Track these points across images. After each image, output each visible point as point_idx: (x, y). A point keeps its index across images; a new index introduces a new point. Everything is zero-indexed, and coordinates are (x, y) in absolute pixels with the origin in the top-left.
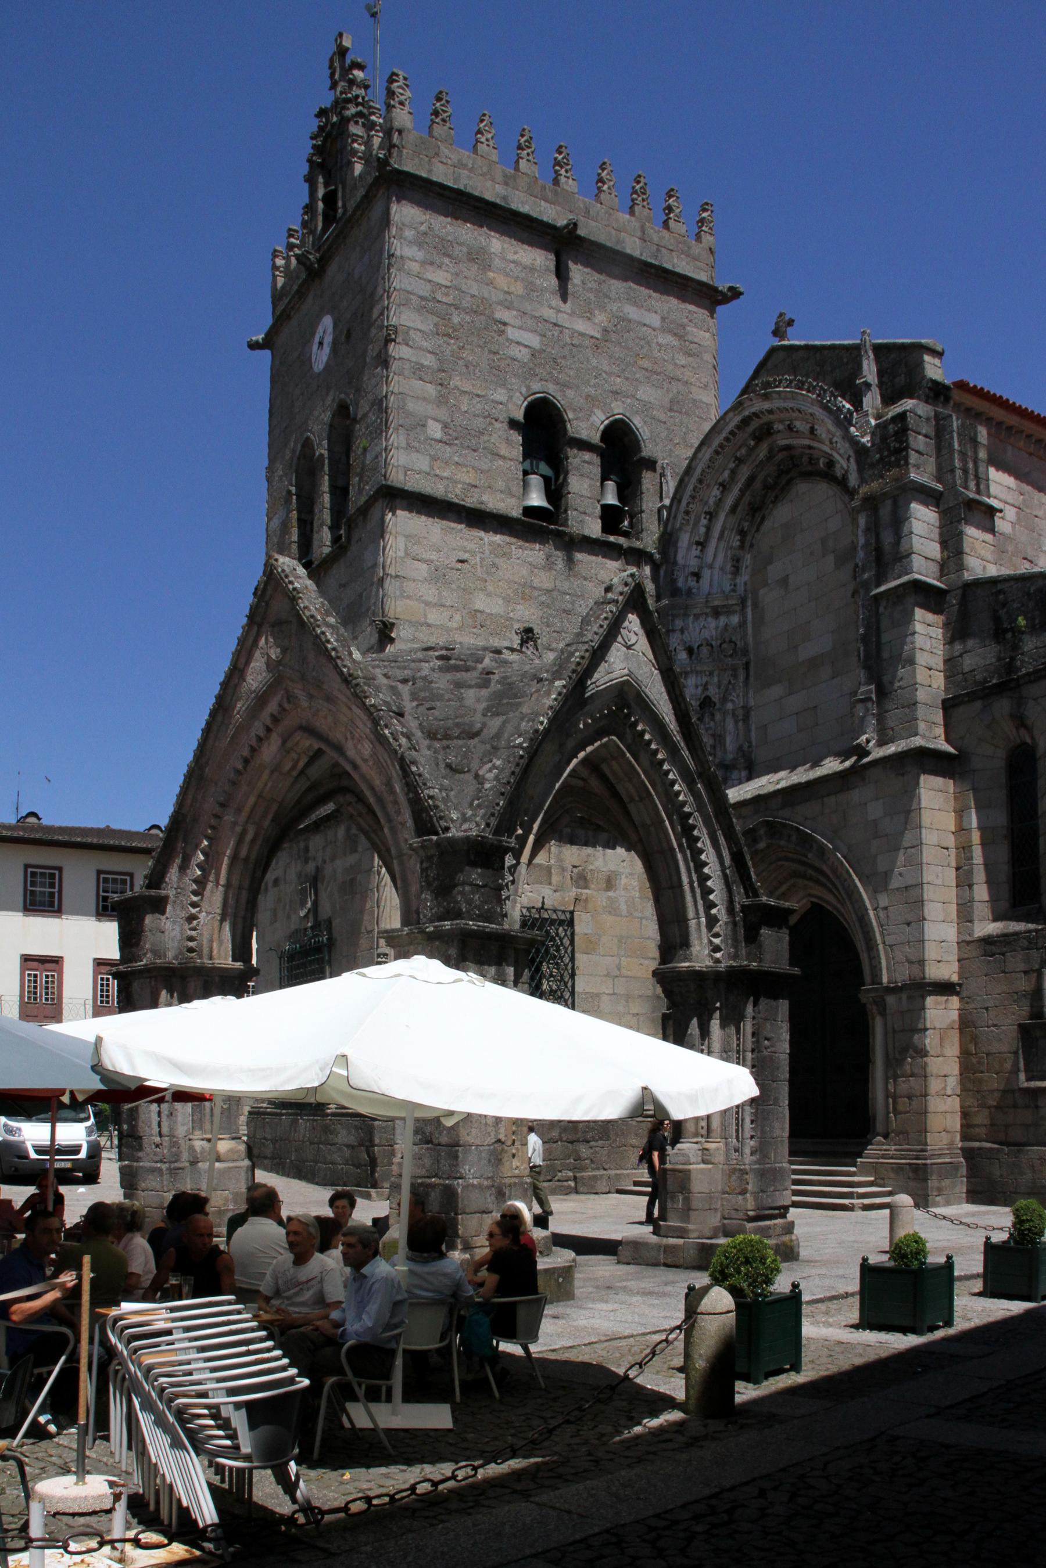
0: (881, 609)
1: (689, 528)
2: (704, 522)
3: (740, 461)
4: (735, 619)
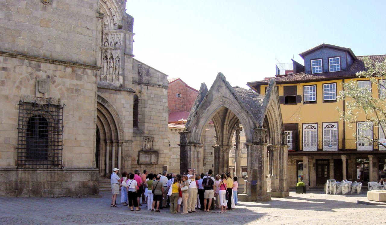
0: (125, 57)
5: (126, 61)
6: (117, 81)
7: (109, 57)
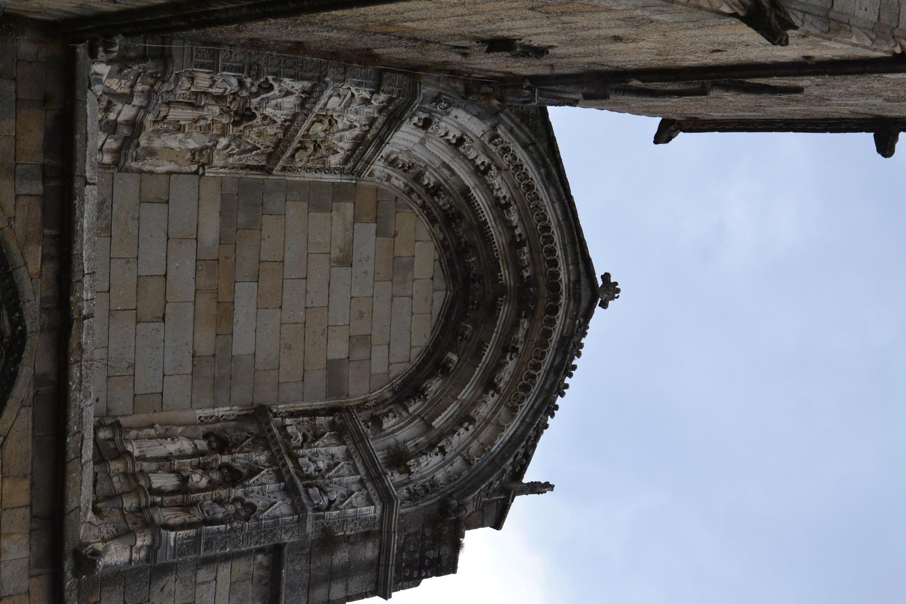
0: (260, 557)
1: (486, 139)
2: (479, 162)
3: (515, 245)
4: (334, 160)
5: (241, 566)
6: (111, 528)
7: (240, 459)
